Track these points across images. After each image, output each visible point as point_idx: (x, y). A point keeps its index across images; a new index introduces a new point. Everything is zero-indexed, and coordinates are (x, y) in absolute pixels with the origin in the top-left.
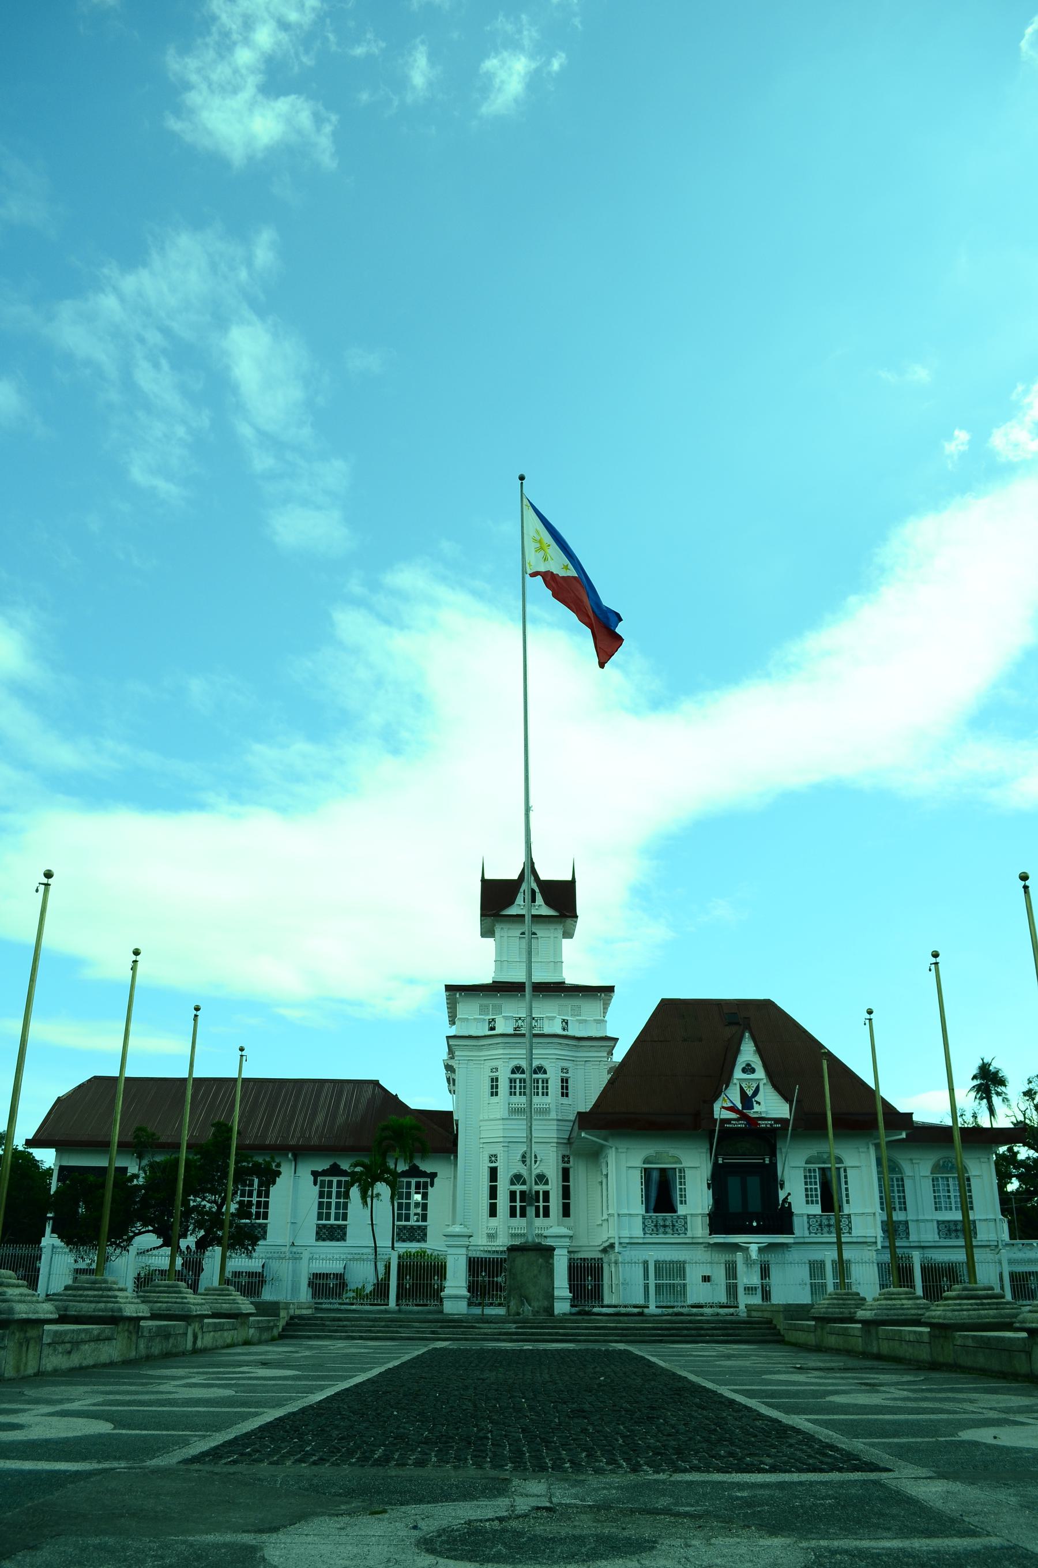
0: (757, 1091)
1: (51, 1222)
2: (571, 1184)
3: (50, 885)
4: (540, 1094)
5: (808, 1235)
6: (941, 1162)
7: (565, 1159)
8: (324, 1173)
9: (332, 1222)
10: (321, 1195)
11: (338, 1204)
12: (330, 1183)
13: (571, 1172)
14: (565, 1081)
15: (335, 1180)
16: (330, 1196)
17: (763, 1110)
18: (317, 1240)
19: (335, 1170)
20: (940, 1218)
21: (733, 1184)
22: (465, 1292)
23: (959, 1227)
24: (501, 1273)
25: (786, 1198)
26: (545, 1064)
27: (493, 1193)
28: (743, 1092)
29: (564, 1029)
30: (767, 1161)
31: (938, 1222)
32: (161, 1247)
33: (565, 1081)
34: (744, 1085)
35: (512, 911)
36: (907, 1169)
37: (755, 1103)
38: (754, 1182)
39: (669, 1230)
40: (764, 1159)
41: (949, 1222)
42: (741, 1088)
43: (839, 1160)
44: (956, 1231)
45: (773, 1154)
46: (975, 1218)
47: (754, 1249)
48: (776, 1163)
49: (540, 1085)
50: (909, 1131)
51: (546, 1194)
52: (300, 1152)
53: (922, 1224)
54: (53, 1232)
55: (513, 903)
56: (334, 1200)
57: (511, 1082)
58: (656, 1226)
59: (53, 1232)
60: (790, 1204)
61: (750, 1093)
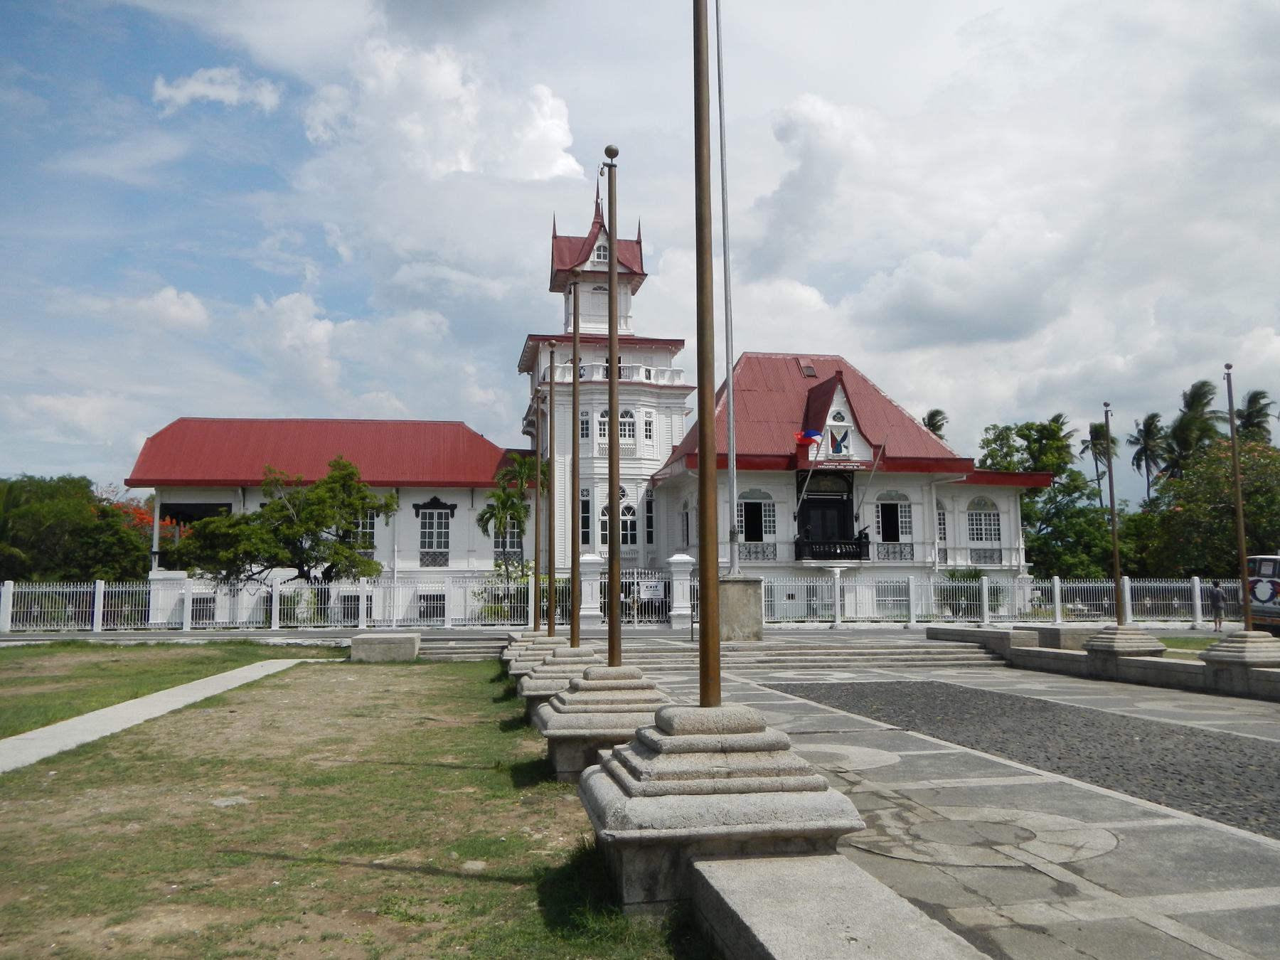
0: (845, 436)
1: (157, 557)
2: (654, 514)
3: (615, 166)
4: (627, 436)
5: (876, 560)
6: (976, 501)
7: (649, 492)
8: (426, 506)
9: (435, 549)
10: (423, 526)
11: (439, 535)
12: (431, 516)
13: (654, 505)
14: (648, 424)
15: (436, 512)
16: (431, 526)
17: (851, 453)
18: (422, 566)
19: (435, 503)
20: (973, 547)
21: (815, 514)
22: (598, 612)
23: (987, 555)
24: (629, 594)
25: (865, 529)
26: (629, 408)
27: (586, 522)
28: (833, 439)
29: (647, 378)
30: (845, 497)
31: (971, 550)
32: (296, 578)
33: (648, 424)
34: (834, 432)
35: (588, 267)
36: (948, 504)
37: (843, 448)
38: (832, 514)
39: (760, 556)
40: (842, 496)
41: (980, 550)
42: (832, 433)
43: (906, 498)
44: (985, 557)
45: (850, 492)
46: (1003, 546)
47: (837, 571)
48: (852, 500)
49: (627, 428)
50: (969, 474)
51: (633, 524)
52: (399, 487)
53: (959, 552)
54: (159, 566)
55: (587, 259)
56: (435, 530)
57: (600, 425)
58: (749, 552)
59: (159, 566)
60: (867, 535)
61: (839, 438)
